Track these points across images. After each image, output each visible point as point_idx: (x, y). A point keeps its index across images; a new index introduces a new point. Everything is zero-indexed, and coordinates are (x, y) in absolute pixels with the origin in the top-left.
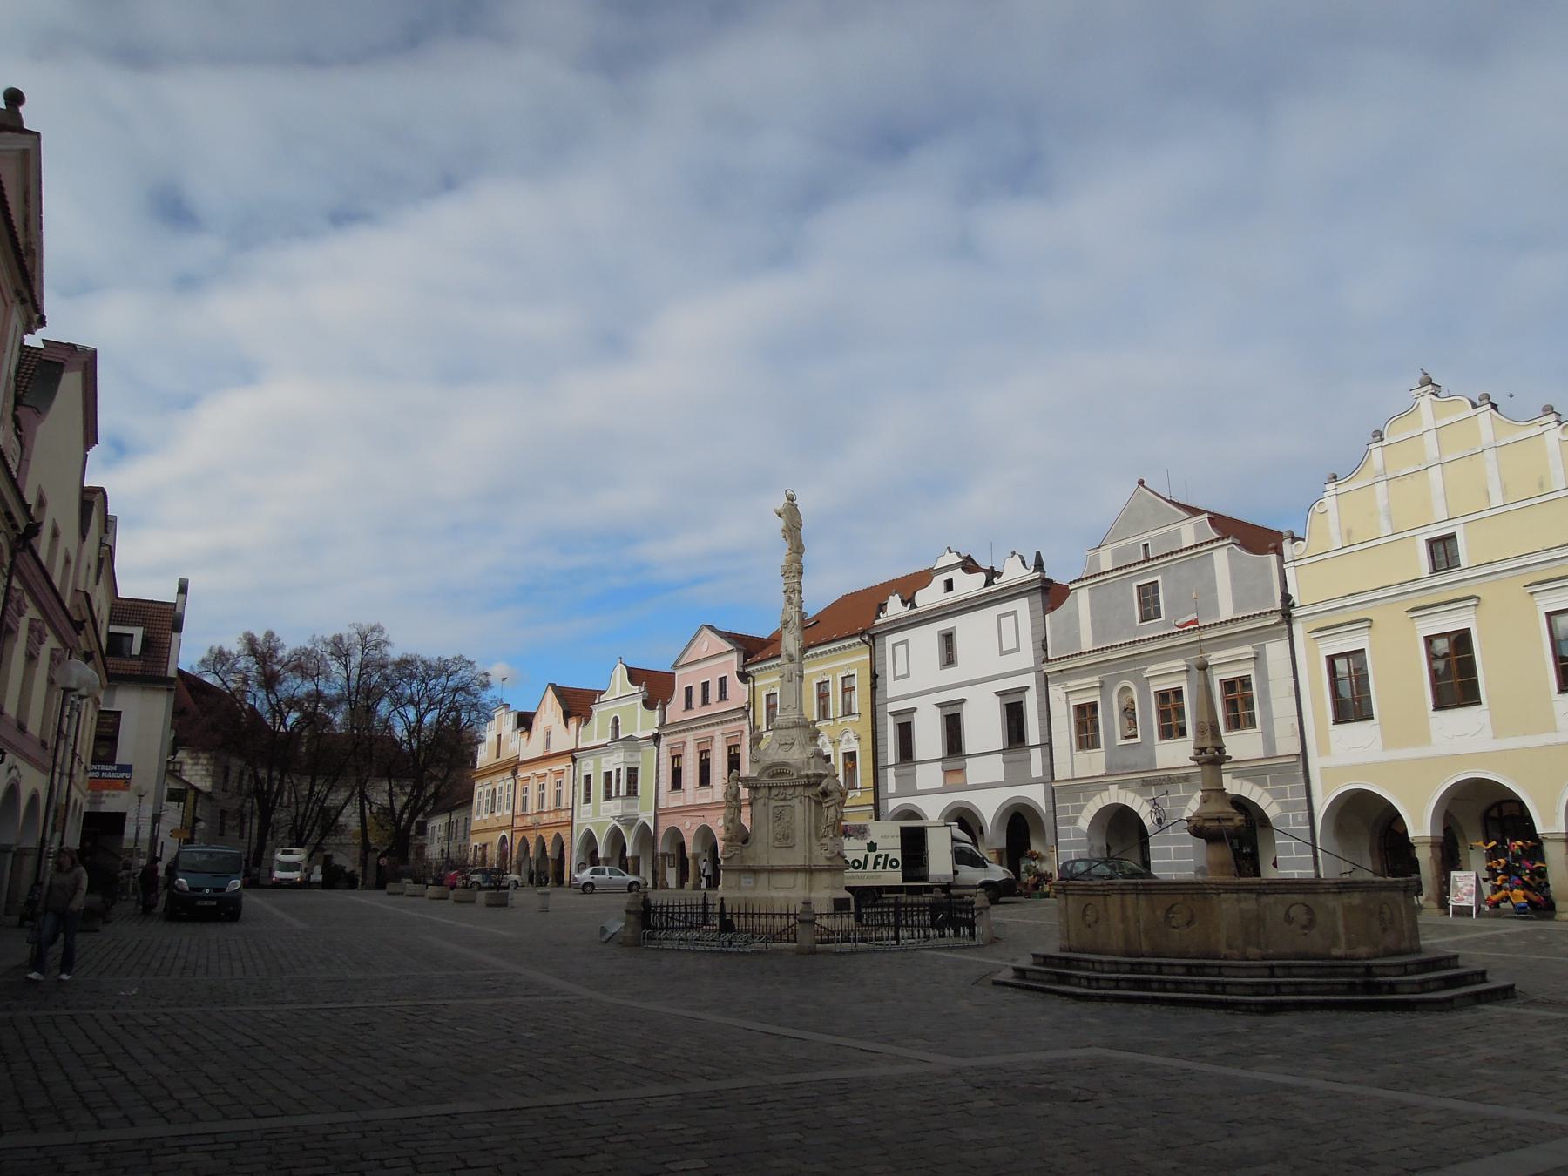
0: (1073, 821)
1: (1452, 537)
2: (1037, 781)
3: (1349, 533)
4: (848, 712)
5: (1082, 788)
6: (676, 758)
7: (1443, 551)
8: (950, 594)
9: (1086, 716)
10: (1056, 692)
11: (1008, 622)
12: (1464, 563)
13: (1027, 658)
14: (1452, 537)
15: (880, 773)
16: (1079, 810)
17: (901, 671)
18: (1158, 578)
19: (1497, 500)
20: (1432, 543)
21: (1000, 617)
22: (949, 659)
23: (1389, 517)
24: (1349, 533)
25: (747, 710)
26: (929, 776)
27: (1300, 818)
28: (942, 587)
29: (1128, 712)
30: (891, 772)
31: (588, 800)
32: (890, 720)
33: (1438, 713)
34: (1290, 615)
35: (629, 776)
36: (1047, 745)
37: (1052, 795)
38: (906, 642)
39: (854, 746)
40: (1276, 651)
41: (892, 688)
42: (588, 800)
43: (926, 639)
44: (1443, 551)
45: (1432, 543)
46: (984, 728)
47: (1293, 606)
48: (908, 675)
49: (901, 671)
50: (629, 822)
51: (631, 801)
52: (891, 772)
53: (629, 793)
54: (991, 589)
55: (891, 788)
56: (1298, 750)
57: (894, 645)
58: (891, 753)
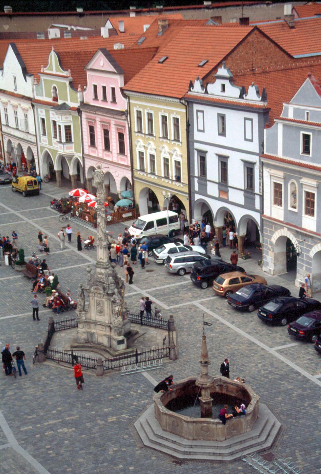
0: (270, 237)
2: (257, 211)
4: (177, 139)
5: (275, 224)
6: (92, 129)
8: (223, 94)
9: (277, 187)
10: (266, 171)
11: (248, 123)
13: (255, 147)
15: (191, 179)
16: (272, 233)
17: (201, 128)
21: (245, 119)
22: (223, 132)
25: (126, 114)
26: (213, 189)
28: (220, 88)
29: (294, 194)
30: (196, 180)
31: (44, 134)
32: (196, 153)
35: (66, 130)
36: (262, 197)
37: (262, 221)
38: (202, 112)
39: (179, 159)
41: (197, 136)
42: (44, 134)
43: (211, 114)
46: (237, 176)
48: (203, 131)
49: (201, 128)
50: (71, 157)
51: (69, 145)
52: (196, 180)
53: (67, 140)
54: (242, 101)
55: (196, 188)
57: (198, 111)
58: (197, 172)
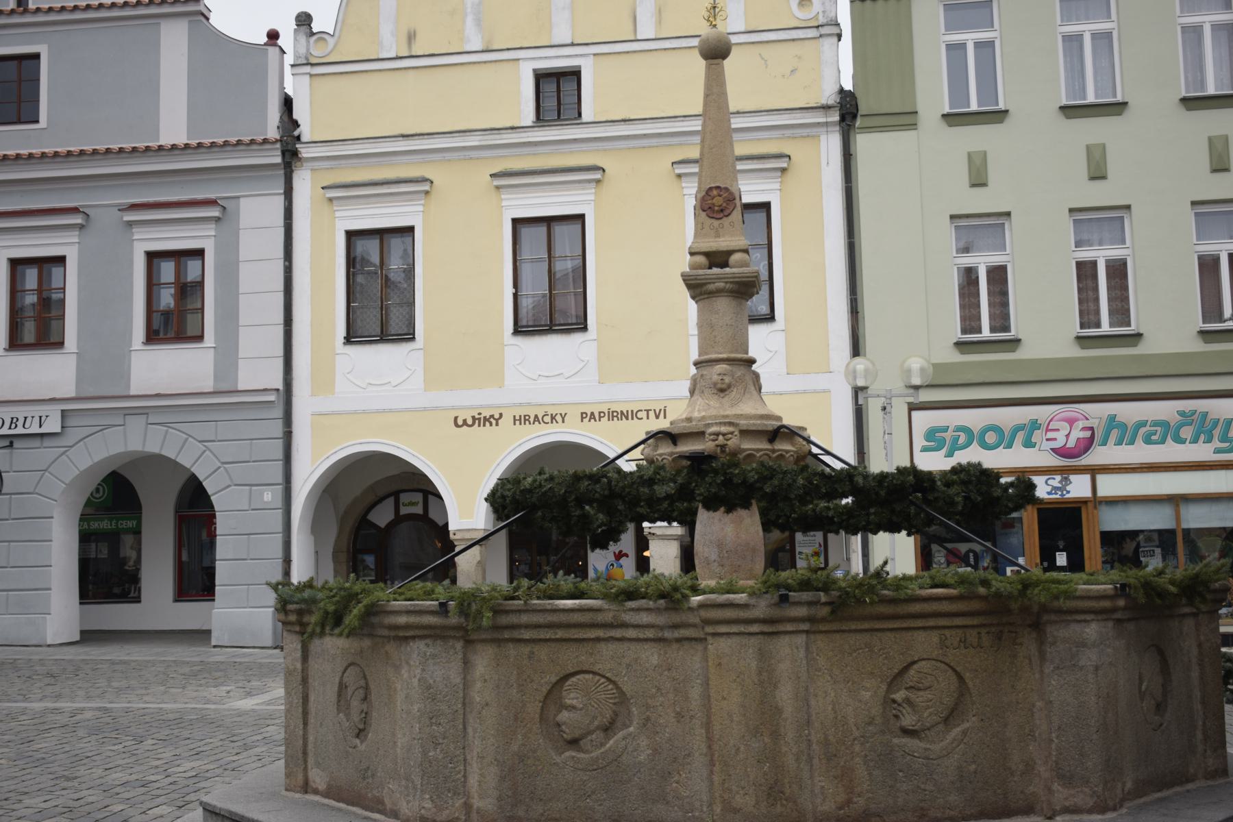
1: (575, 74)
3: (411, 37)
7: (558, 91)
12: (587, 115)
14: (575, 74)
18: (42, 49)
19: (646, 30)
20: (541, 77)
23: (479, 22)
24: (411, 37)
27: (268, 496)
33: (522, 341)
34: (295, 154)
40: (258, 211)
44: (558, 91)
45: (541, 77)
47: (298, 138)
56: (279, 385)
